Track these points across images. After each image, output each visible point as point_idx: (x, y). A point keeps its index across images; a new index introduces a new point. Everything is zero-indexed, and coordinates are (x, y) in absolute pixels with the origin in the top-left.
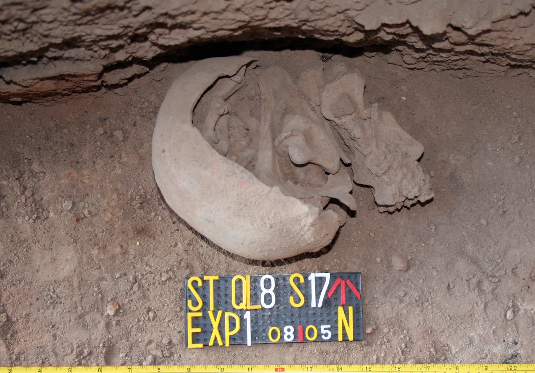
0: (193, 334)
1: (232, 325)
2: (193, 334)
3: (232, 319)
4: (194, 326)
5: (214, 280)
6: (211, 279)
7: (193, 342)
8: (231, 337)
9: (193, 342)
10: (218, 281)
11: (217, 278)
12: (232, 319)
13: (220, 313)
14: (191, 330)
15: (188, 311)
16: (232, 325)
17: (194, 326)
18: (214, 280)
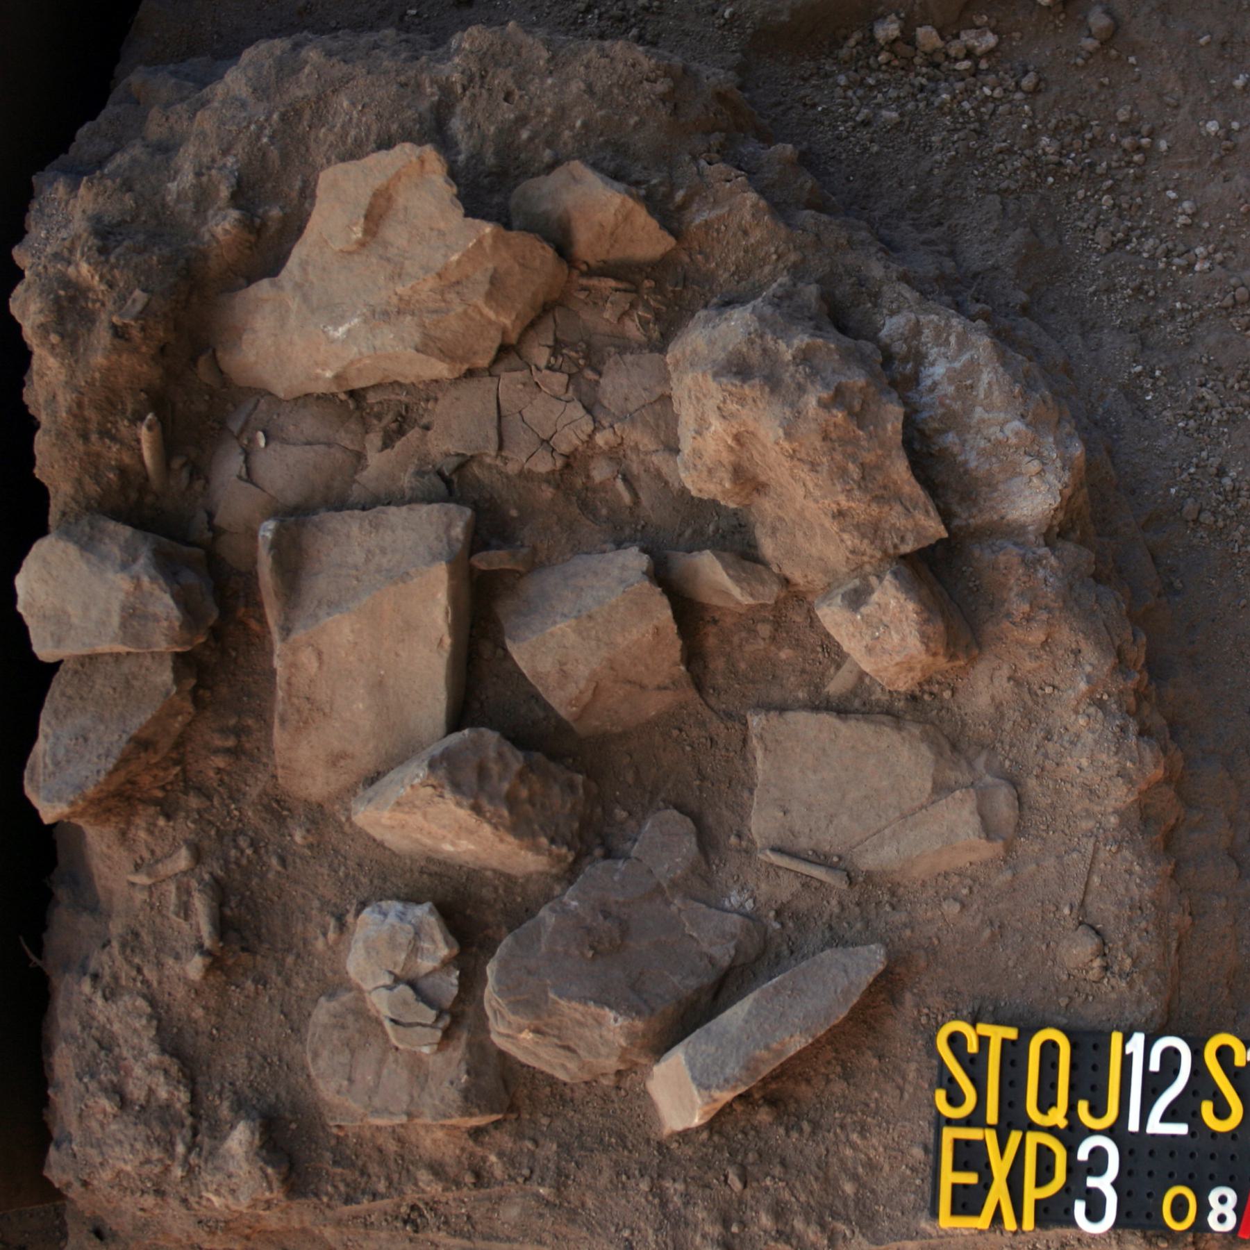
0: (955, 1187)
1: (1045, 1174)
2: (955, 1187)
3: (1044, 1154)
4: (956, 1167)
5: (1004, 1041)
7: (955, 1211)
8: (1038, 1202)
9: (955, 1211)
10: (1013, 1042)
11: (1012, 1033)
12: (1044, 1154)
13: (1015, 1137)
14: (949, 1177)
15: (943, 1121)
16: (1045, 1174)
17: (956, 1167)
18: (1004, 1042)
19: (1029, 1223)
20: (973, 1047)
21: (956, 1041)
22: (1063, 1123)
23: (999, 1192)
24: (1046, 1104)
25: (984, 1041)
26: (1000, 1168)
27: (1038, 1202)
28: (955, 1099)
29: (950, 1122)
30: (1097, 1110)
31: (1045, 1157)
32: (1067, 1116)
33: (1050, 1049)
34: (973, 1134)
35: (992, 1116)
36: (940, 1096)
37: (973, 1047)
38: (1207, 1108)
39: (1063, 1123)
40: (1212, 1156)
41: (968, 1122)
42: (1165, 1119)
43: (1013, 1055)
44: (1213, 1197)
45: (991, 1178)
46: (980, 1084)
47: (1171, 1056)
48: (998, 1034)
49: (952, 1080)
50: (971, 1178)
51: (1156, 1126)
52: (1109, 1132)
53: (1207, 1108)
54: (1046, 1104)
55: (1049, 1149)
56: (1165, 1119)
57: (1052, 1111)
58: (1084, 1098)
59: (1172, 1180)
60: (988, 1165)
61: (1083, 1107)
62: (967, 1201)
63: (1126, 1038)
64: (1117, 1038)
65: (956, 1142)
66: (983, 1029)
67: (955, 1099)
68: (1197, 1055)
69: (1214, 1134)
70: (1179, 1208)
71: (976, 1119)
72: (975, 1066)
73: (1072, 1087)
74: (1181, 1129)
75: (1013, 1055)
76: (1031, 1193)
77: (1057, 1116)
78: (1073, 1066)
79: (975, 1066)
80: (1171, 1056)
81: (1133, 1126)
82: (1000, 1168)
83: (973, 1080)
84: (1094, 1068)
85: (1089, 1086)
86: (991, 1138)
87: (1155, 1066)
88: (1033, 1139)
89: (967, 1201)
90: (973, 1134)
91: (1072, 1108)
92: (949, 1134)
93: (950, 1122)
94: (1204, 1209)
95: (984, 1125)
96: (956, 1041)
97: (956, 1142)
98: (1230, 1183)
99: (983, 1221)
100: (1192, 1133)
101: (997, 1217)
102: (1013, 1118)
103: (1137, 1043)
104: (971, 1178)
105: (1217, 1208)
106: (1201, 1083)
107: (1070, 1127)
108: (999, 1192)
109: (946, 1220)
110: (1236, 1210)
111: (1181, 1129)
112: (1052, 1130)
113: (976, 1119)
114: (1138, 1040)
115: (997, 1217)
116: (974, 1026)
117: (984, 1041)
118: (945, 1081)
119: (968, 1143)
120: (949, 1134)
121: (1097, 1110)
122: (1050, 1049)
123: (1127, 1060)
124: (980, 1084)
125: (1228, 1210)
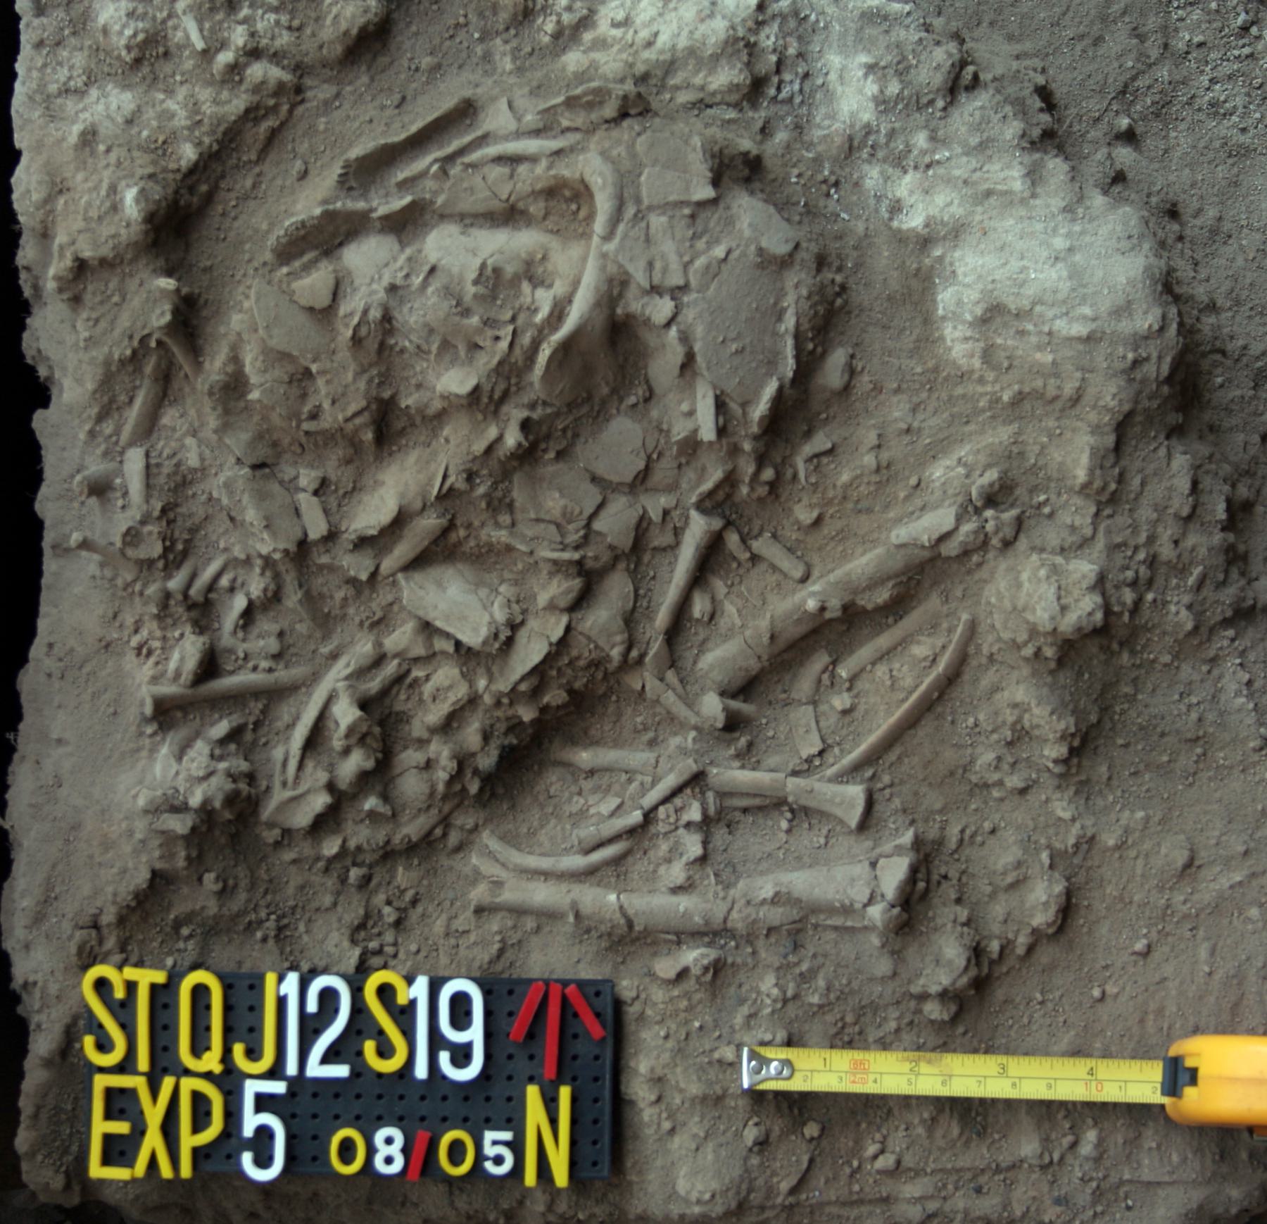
0: (108, 1139)
1: (200, 1119)
4: (109, 1116)
5: (154, 988)
6: (147, 977)
7: (106, 1161)
8: (196, 1151)
9: (106, 1161)
10: (165, 986)
11: (160, 977)
12: (197, 1097)
13: (168, 1083)
14: (100, 1127)
16: (200, 1119)
17: (109, 1116)
18: (154, 988)
19: (186, 1171)
20: (119, 993)
21: (102, 985)
22: (217, 1068)
23: (153, 1140)
24: (199, 1048)
25: (131, 987)
26: (154, 1115)
27: (196, 1151)
28: (104, 1045)
29: (102, 1070)
30: (253, 1053)
31: (200, 1102)
33: (200, 992)
35: (143, 1063)
37: (119, 993)
38: (369, 1047)
39: (217, 1068)
43: (162, 997)
46: (128, 1028)
47: (328, 996)
48: (147, 977)
49: (101, 1026)
50: (122, 1127)
51: (315, 1069)
53: (369, 1047)
54: (199, 1048)
57: (207, 1055)
58: (240, 1041)
59: (338, 1120)
60: (142, 1113)
61: (238, 1049)
62: (117, 1151)
63: (281, 979)
64: (271, 978)
66: (130, 973)
67: (104, 1045)
69: (380, 1075)
70: (347, 1150)
71: (125, 1067)
72: (123, 1011)
73: (228, 1030)
74: (341, 1071)
75: (162, 997)
76: (188, 1141)
77: (211, 1061)
78: (228, 1008)
81: (292, 1069)
82: (154, 1115)
83: (123, 1026)
87: (312, 1007)
88: (188, 1084)
93: (102, 1070)
94: (371, 1150)
95: (135, 1072)
96: (102, 985)
98: (399, 1121)
100: (355, 1074)
101: (153, 1163)
102: (164, 1063)
103: (291, 985)
104: (122, 1127)
105: (383, 1151)
106: (360, 1021)
108: (153, 1140)
109: (97, 1170)
110: (405, 1150)
111: (341, 1071)
112: (208, 1076)
113: (125, 1067)
114: (292, 980)
115: (153, 1163)
116: (120, 968)
117: (131, 987)
119: (122, 1091)
120: (101, 1082)
121: (253, 1053)
122: (200, 992)
123: (282, 1002)
124: (128, 1028)
125: (395, 1150)
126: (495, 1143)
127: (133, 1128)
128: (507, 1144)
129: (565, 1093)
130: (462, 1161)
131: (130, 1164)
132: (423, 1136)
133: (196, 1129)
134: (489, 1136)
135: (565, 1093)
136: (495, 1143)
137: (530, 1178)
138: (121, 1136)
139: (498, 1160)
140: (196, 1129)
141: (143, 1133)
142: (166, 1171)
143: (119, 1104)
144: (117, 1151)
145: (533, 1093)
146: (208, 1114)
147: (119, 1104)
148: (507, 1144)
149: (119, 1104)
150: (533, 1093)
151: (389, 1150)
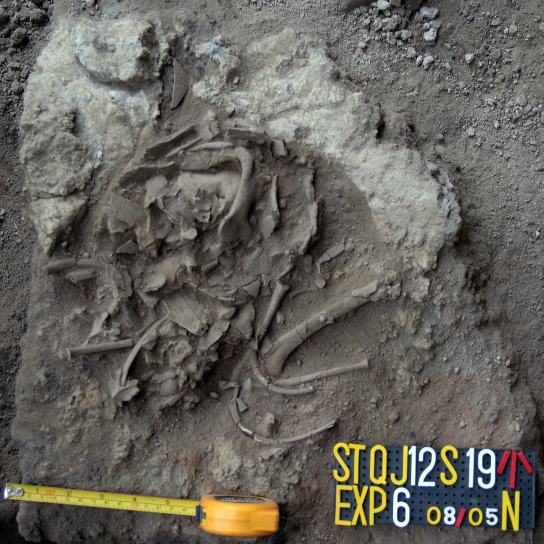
0: (342, 509)
1: (378, 502)
2: (342, 509)
4: (342, 501)
5: (360, 451)
6: (358, 448)
7: (341, 518)
8: (375, 515)
9: (341, 518)
10: (364, 451)
11: (363, 447)
12: (377, 494)
13: (365, 488)
14: (339, 505)
16: (378, 502)
17: (342, 501)
18: (360, 451)
19: (372, 522)
21: (341, 450)
22: (384, 483)
23: (359, 510)
24: (377, 475)
25: (352, 451)
26: (360, 501)
27: (375, 515)
29: (340, 483)
30: (398, 477)
32: (386, 480)
33: (378, 453)
34: (348, 488)
35: (356, 480)
36: (335, 472)
37: (348, 453)
38: (442, 475)
39: (384, 483)
40: (446, 495)
41: (347, 483)
42: (426, 480)
44: (446, 510)
45: (356, 505)
47: (427, 455)
48: (358, 448)
49: (340, 466)
50: (347, 505)
51: (422, 483)
52: (404, 486)
53: (442, 475)
54: (377, 475)
55: (379, 494)
56: (426, 480)
57: (380, 478)
60: (355, 500)
61: (393, 476)
63: (409, 448)
64: (405, 448)
65: (342, 492)
66: (352, 446)
68: (438, 454)
69: (446, 486)
70: (433, 515)
72: (349, 460)
73: (388, 468)
74: (432, 484)
75: (364, 455)
76: (373, 511)
77: (382, 480)
78: (388, 460)
79: (349, 460)
80: (427, 455)
81: (413, 483)
82: (360, 501)
83: (348, 467)
84: (397, 460)
85: (394, 466)
86: (356, 488)
87: (421, 459)
88: (373, 489)
89: (346, 514)
90: (348, 488)
91: (388, 476)
92: (339, 488)
93: (340, 483)
94: (443, 515)
96: (341, 450)
97: (342, 492)
98: (454, 504)
99: (354, 522)
100: (437, 486)
102: (364, 481)
104: (347, 505)
105: (447, 515)
107: (388, 484)
108: (359, 510)
109: (338, 522)
110: (456, 516)
111: (432, 484)
112: (380, 486)
114: (413, 449)
116: (348, 444)
117: (352, 451)
118: (337, 467)
119: (347, 491)
120: (339, 488)
122: (378, 453)
123: (409, 457)
125: (452, 516)
126: (491, 513)
127: (351, 506)
128: (495, 513)
129: (517, 494)
130: (478, 520)
131: (351, 520)
132: (463, 511)
133: (376, 506)
134: (488, 510)
135: (517, 494)
136: (491, 513)
137: (504, 527)
138: (347, 509)
139: (492, 520)
140: (376, 506)
141: (355, 508)
142: (364, 522)
143: (346, 496)
144: (346, 514)
145: (505, 494)
146: (380, 501)
147: (346, 496)
148: (495, 513)
149: (346, 496)
150: (505, 494)
151: (450, 515)
